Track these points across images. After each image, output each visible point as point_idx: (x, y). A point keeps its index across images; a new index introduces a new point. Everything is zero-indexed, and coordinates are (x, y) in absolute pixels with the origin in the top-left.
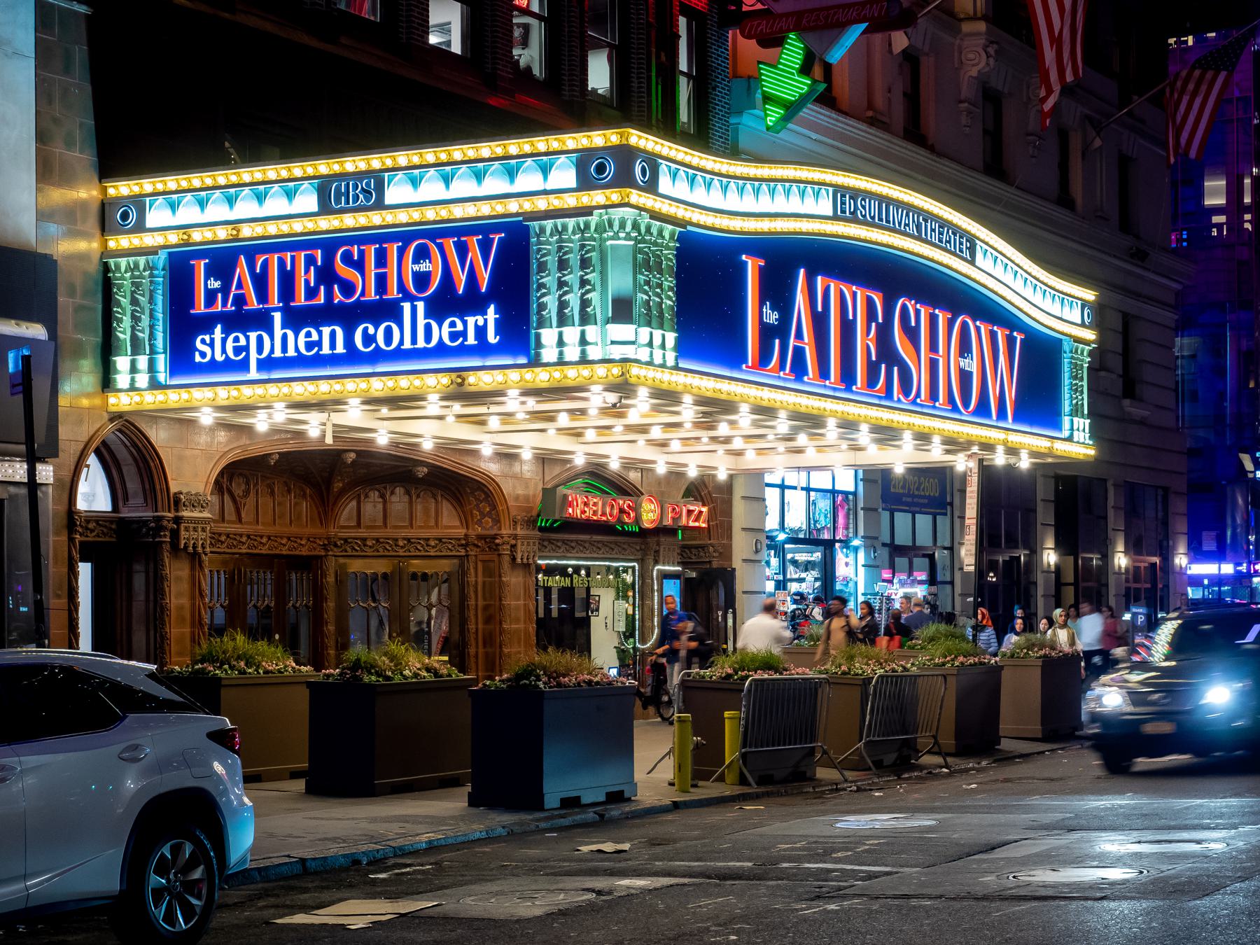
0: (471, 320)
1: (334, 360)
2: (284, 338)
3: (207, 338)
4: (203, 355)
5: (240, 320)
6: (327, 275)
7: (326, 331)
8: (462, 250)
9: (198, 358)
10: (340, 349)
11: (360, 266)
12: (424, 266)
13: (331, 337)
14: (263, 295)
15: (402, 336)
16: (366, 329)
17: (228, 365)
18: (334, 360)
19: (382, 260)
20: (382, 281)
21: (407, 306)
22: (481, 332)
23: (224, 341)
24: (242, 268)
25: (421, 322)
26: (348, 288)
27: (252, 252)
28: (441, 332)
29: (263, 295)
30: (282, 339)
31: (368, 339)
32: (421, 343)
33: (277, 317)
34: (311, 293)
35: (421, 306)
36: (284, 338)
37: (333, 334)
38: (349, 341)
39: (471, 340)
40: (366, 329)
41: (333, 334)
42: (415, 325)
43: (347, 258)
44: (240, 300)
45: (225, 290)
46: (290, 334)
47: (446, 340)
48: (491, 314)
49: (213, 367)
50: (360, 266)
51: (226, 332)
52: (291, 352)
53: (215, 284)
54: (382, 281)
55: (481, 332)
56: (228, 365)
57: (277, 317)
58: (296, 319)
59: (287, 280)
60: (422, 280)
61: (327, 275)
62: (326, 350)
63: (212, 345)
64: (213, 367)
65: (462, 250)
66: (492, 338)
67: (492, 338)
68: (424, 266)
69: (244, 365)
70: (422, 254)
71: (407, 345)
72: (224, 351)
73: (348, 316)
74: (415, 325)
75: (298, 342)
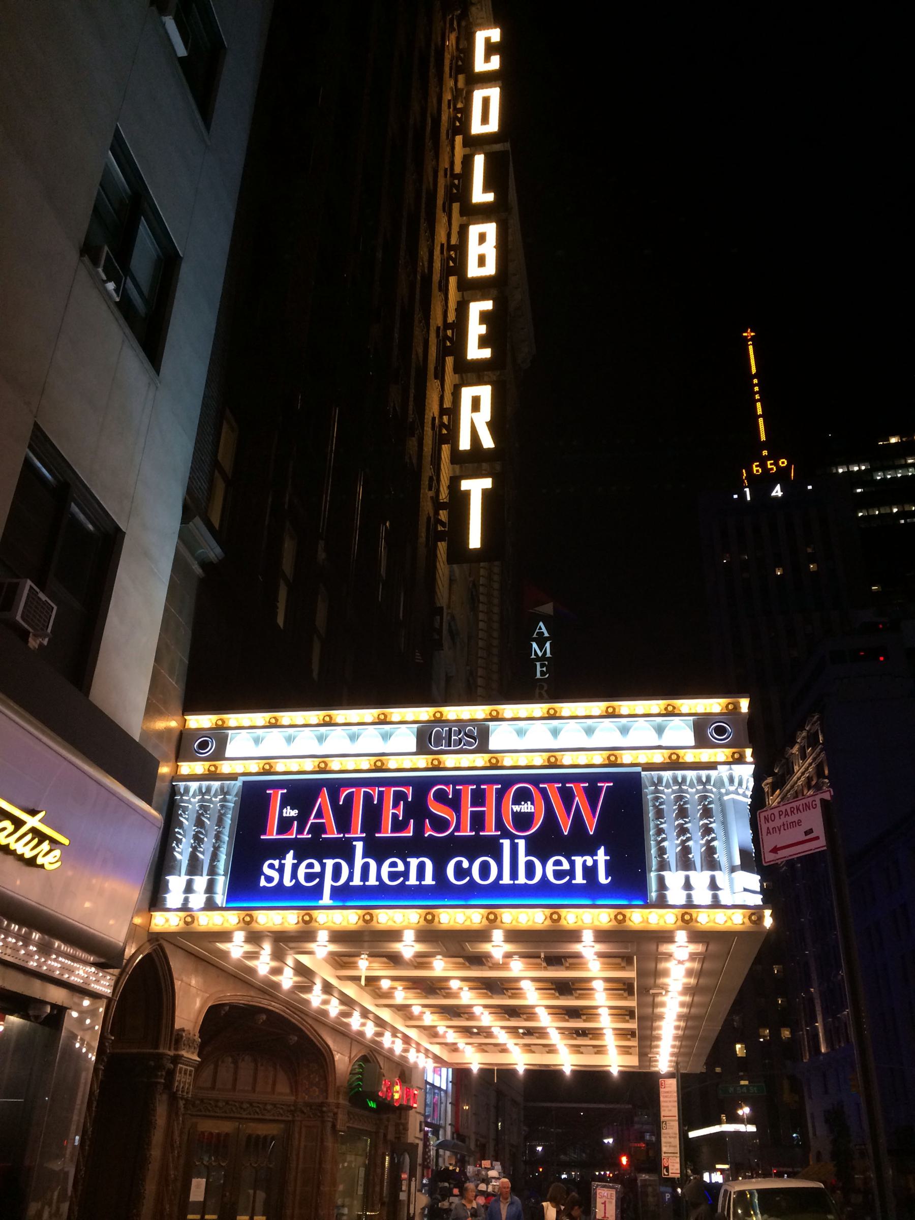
0: (579, 860)
1: (420, 892)
2: (365, 868)
3: (276, 863)
4: (269, 879)
5: (315, 848)
6: (417, 810)
7: (414, 862)
9: (263, 883)
10: (429, 880)
11: (455, 804)
12: (526, 807)
13: (419, 869)
16: (459, 864)
17: (297, 892)
18: (420, 892)
19: (479, 798)
20: (478, 821)
21: (506, 843)
22: (590, 872)
23: (295, 868)
25: (522, 859)
26: (440, 824)
29: (344, 823)
30: (363, 869)
31: (460, 872)
32: (522, 879)
33: (359, 846)
34: (398, 825)
35: (521, 844)
36: (365, 868)
37: (421, 868)
38: (439, 873)
39: (579, 879)
40: (459, 864)
41: (421, 868)
42: (515, 861)
43: (441, 797)
47: (550, 876)
48: (601, 856)
49: (279, 893)
50: (455, 804)
51: (299, 858)
52: (372, 881)
54: (478, 821)
55: (590, 872)
56: (297, 892)
57: (359, 846)
58: (378, 850)
60: (523, 821)
61: (417, 810)
62: (413, 880)
63: (281, 870)
64: (279, 893)
66: (603, 879)
67: (603, 879)
68: (526, 807)
69: (317, 893)
70: (522, 796)
71: (506, 880)
72: (294, 875)
73: (440, 852)
74: (515, 861)
75: (382, 872)
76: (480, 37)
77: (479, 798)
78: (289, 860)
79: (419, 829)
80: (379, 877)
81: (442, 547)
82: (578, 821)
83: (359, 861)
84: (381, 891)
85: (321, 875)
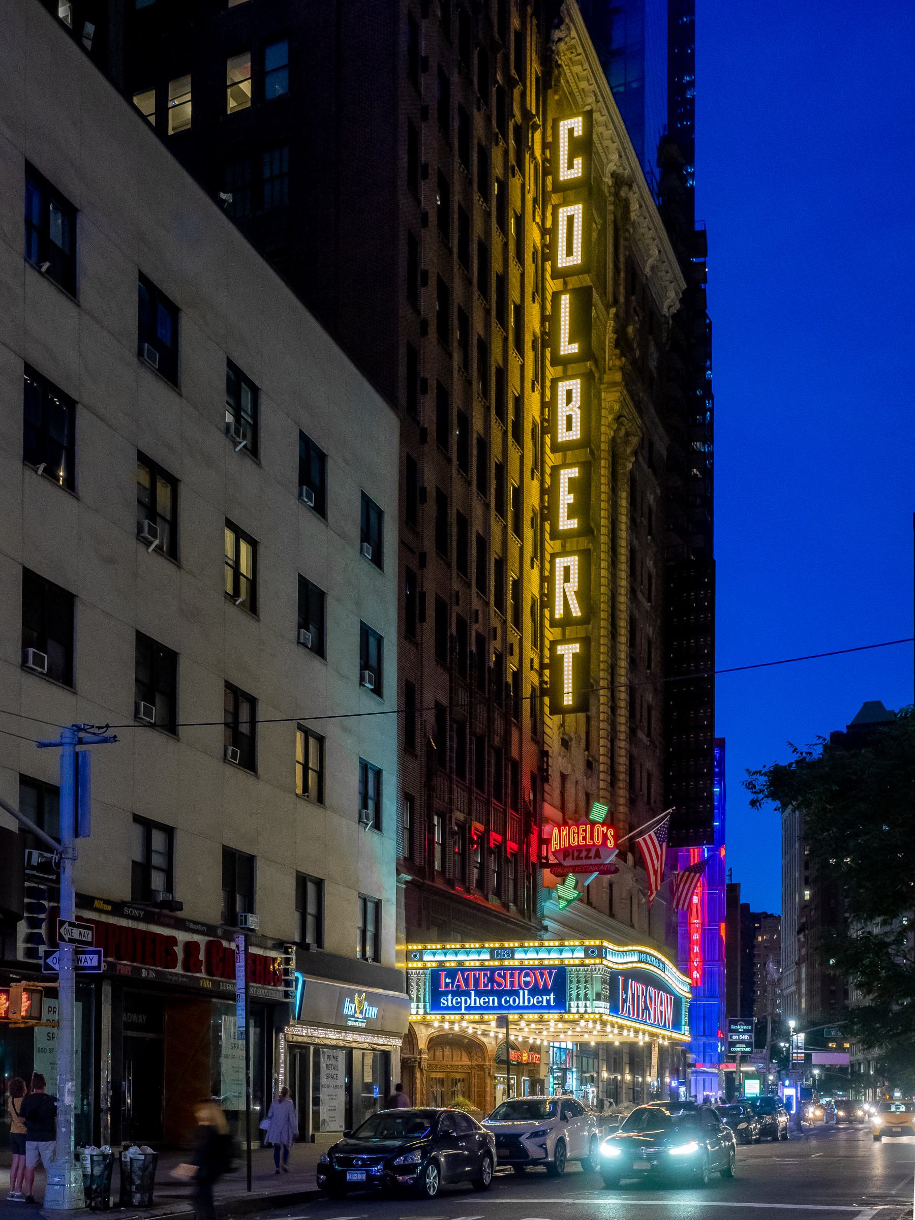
0: (545, 998)
5: (458, 993)
6: (491, 980)
7: (491, 998)
8: (542, 975)
10: (496, 1004)
11: (504, 977)
12: (528, 979)
13: (493, 1001)
14: (467, 985)
17: (453, 1008)
19: (512, 976)
20: (512, 983)
21: (521, 992)
22: (548, 1001)
25: (526, 997)
26: (499, 985)
27: (463, 971)
29: (467, 985)
30: (473, 1000)
31: (506, 1002)
32: (526, 1004)
33: (473, 993)
34: (486, 986)
35: (526, 992)
36: (475, 1000)
37: (493, 1000)
38: (500, 1002)
39: (545, 1004)
41: (493, 1000)
42: (524, 997)
43: (499, 975)
45: (453, 983)
51: (453, 996)
52: (478, 1005)
53: (448, 980)
54: (512, 983)
55: (548, 1001)
56: (453, 1008)
57: (473, 993)
58: (479, 994)
59: (477, 981)
60: (527, 984)
61: (491, 980)
63: (447, 1001)
66: (552, 1004)
68: (528, 979)
69: (460, 1008)
70: (527, 975)
71: (521, 1004)
73: (499, 994)
74: (524, 997)
75: (480, 1002)
77: (512, 976)
78: (450, 997)
79: (492, 986)
83: (473, 998)
84: (481, 1008)
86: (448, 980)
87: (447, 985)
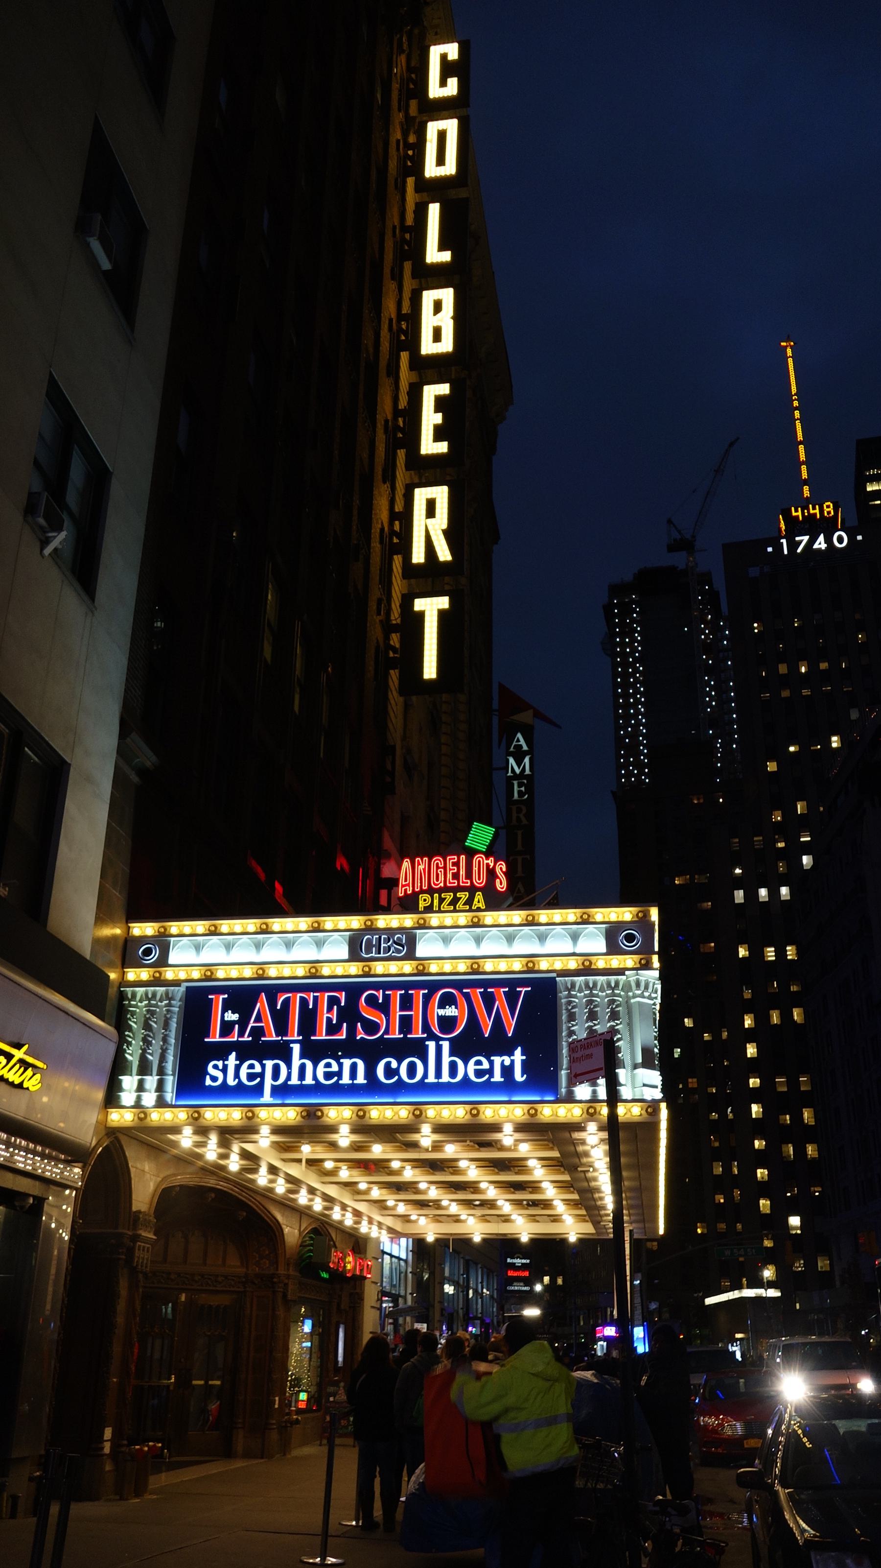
0: (497, 1060)
1: (353, 1089)
2: (302, 1068)
3: (220, 1064)
4: (214, 1079)
6: (350, 1014)
7: (347, 1063)
8: (489, 1001)
9: (208, 1082)
10: (361, 1079)
11: (384, 1008)
12: (450, 1011)
13: (352, 1069)
15: (426, 1072)
16: (388, 1065)
17: (240, 1090)
18: (353, 1089)
20: (406, 1024)
21: (432, 1045)
22: (507, 1071)
23: (237, 1068)
24: (262, 1004)
25: (446, 1059)
27: (273, 992)
28: (469, 1069)
29: (282, 1027)
30: (299, 1068)
31: (390, 1072)
32: (446, 1078)
33: (296, 1048)
34: (332, 1029)
35: (446, 1045)
36: (302, 1068)
37: (354, 1067)
38: (370, 1072)
39: (497, 1077)
40: (388, 1065)
41: (354, 1067)
42: (439, 1061)
43: (372, 1001)
44: (258, 1032)
45: (243, 1023)
46: (309, 1065)
48: (518, 1056)
49: (224, 1090)
50: (384, 1008)
51: (241, 1059)
52: (309, 1080)
53: (231, 1016)
54: (406, 1024)
55: (507, 1071)
56: (240, 1090)
57: (296, 1048)
58: (314, 1052)
59: (309, 1018)
60: (447, 1024)
61: (350, 1014)
62: (346, 1080)
63: (225, 1070)
64: (224, 1090)
65: (489, 1001)
66: (519, 1077)
67: (519, 1077)
68: (450, 1011)
69: (258, 1090)
71: (431, 1079)
72: (237, 1075)
73: (371, 1053)
74: (439, 1061)
75: (318, 1072)
76: (435, 52)
79: (352, 1031)
80: (315, 1077)
81: (394, 674)
82: (498, 1023)
83: (296, 1062)
84: (317, 1088)
85: (262, 1075)
86: (231, 1016)
87: (227, 1028)
